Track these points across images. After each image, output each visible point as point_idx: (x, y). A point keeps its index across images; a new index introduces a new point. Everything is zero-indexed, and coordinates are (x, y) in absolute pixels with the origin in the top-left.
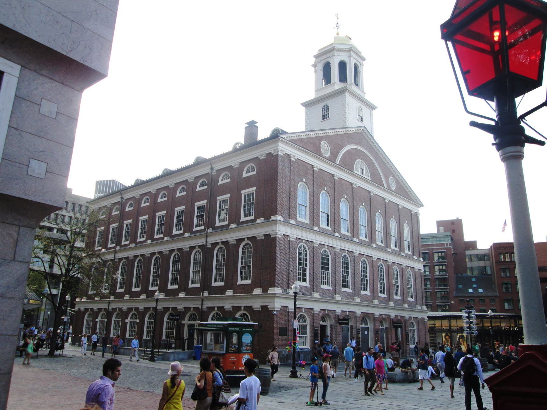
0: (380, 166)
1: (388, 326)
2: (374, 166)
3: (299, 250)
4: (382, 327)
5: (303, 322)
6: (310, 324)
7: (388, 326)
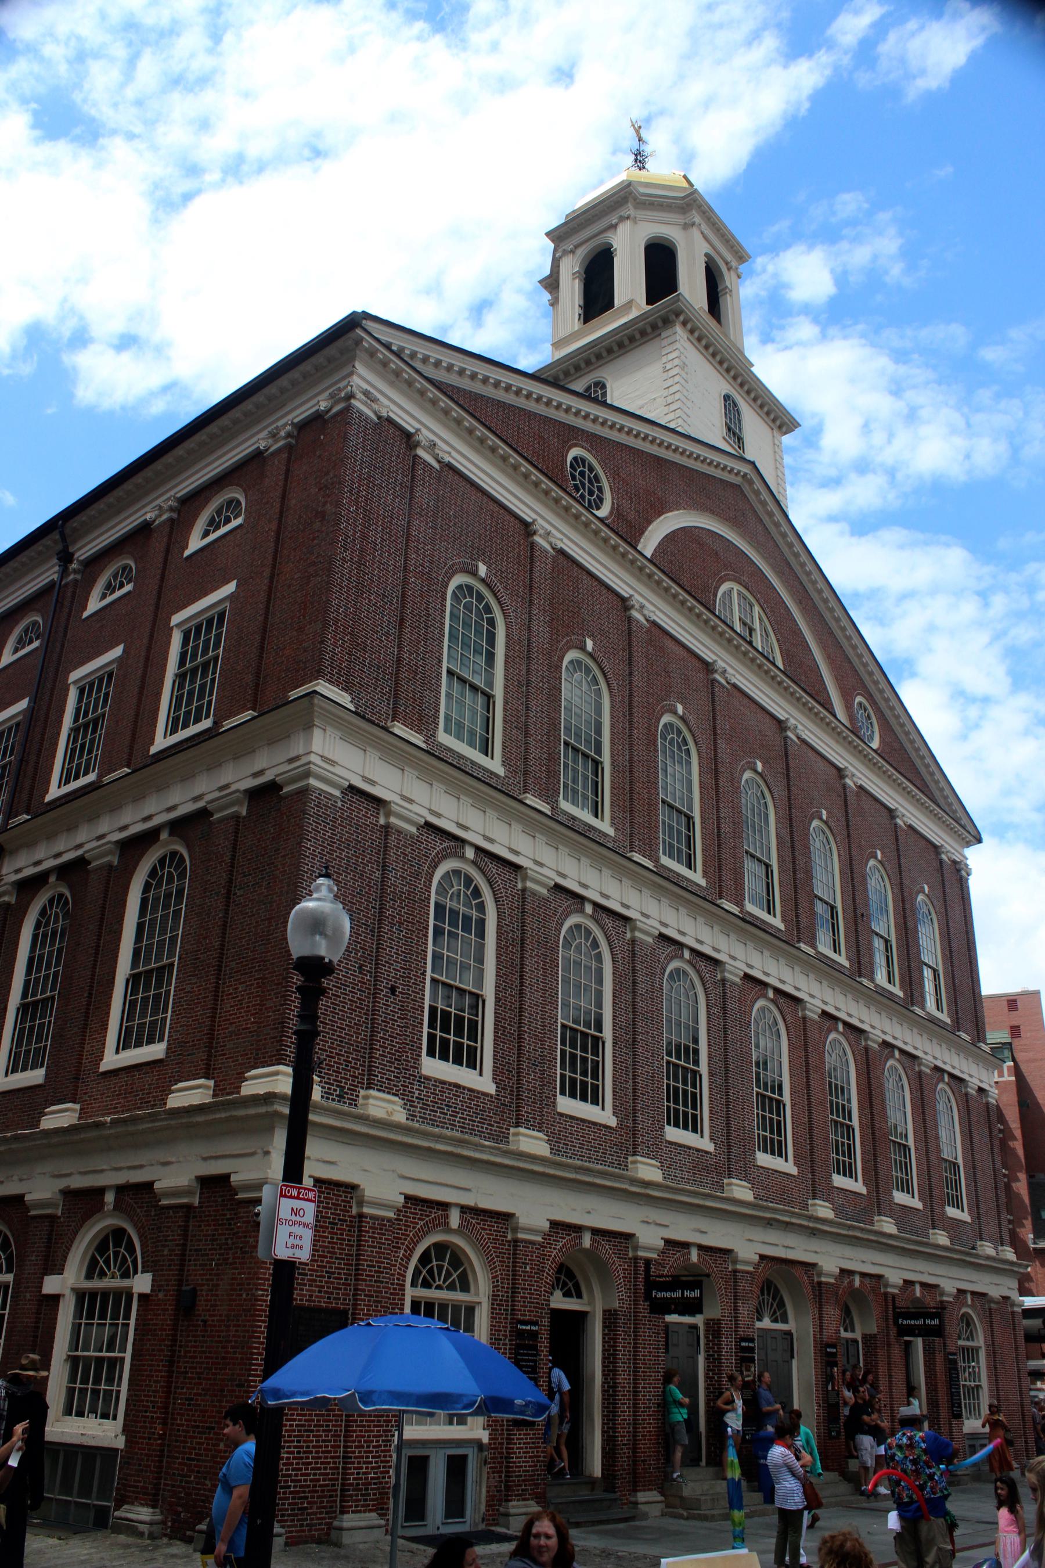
0: (821, 642)
1: (874, 1330)
2: (798, 633)
3: (442, 890)
4: (849, 1335)
5: (451, 1287)
6: (494, 1297)
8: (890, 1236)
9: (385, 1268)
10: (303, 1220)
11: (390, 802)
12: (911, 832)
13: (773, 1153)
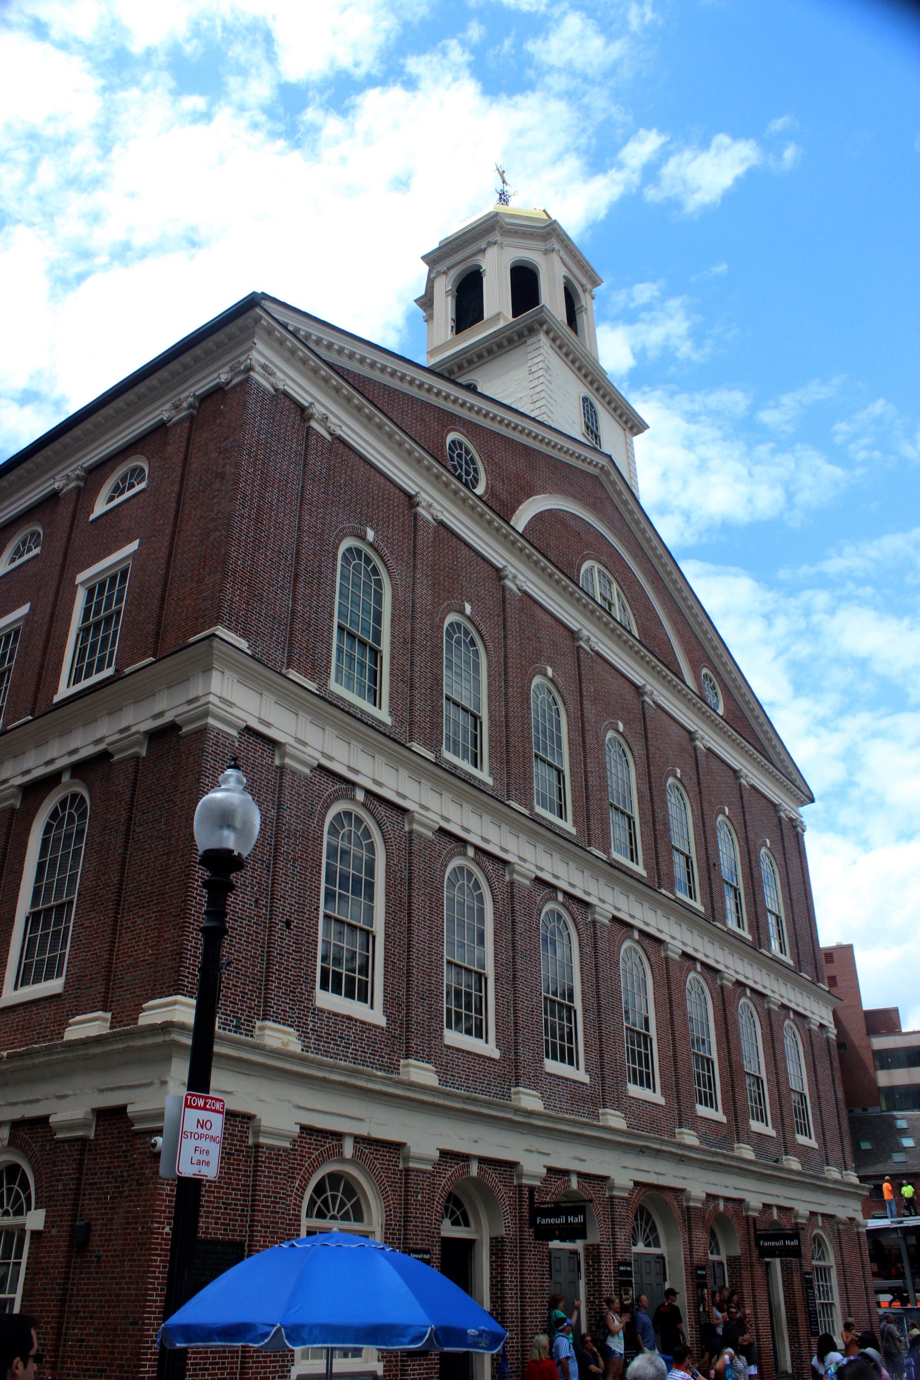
0: (670, 617)
2: (651, 608)
3: (334, 831)
7: (737, 1251)
8: (750, 1162)
9: (281, 1198)
10: (210, 1133)
11: (285, 744)
12: (753, 791)
13: (642, 1085)
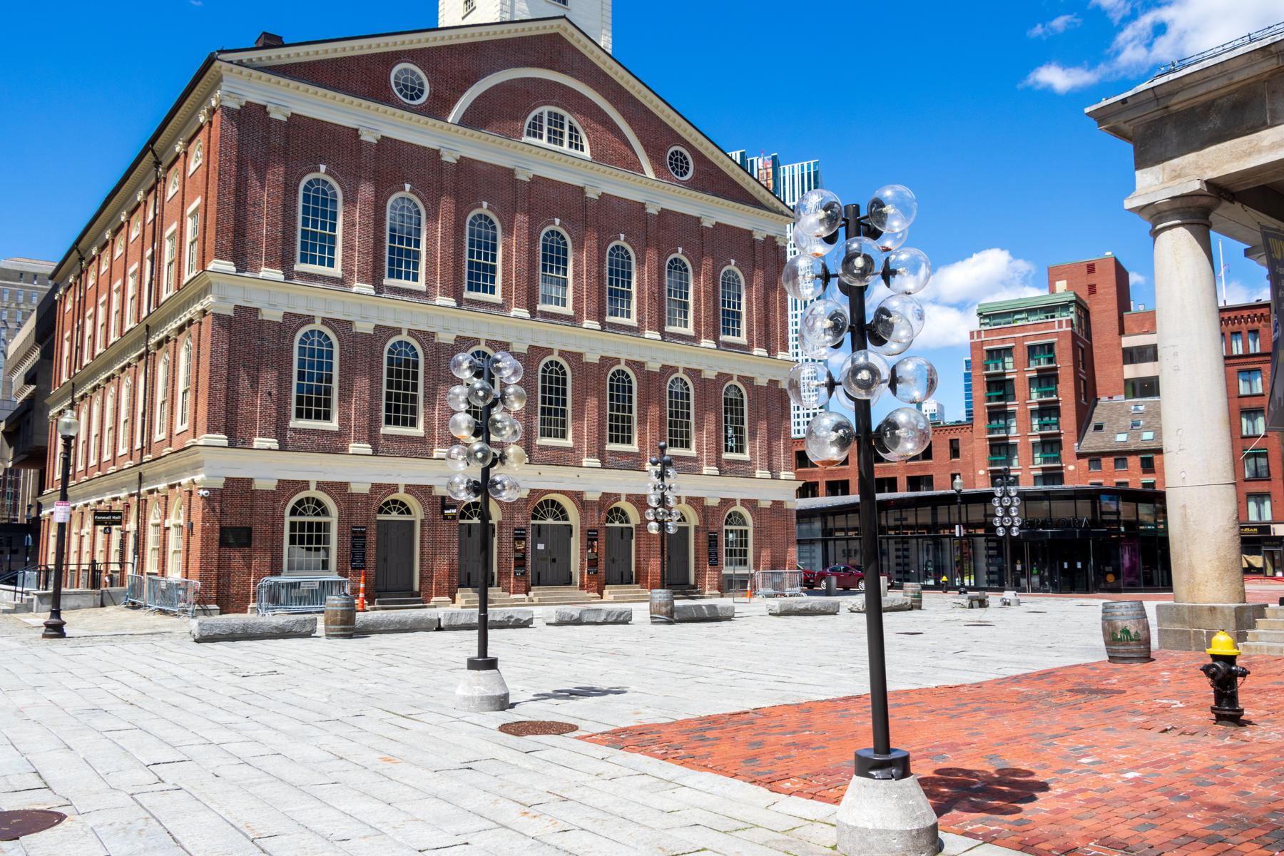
5: (318, 514)
6: (340, 518)
